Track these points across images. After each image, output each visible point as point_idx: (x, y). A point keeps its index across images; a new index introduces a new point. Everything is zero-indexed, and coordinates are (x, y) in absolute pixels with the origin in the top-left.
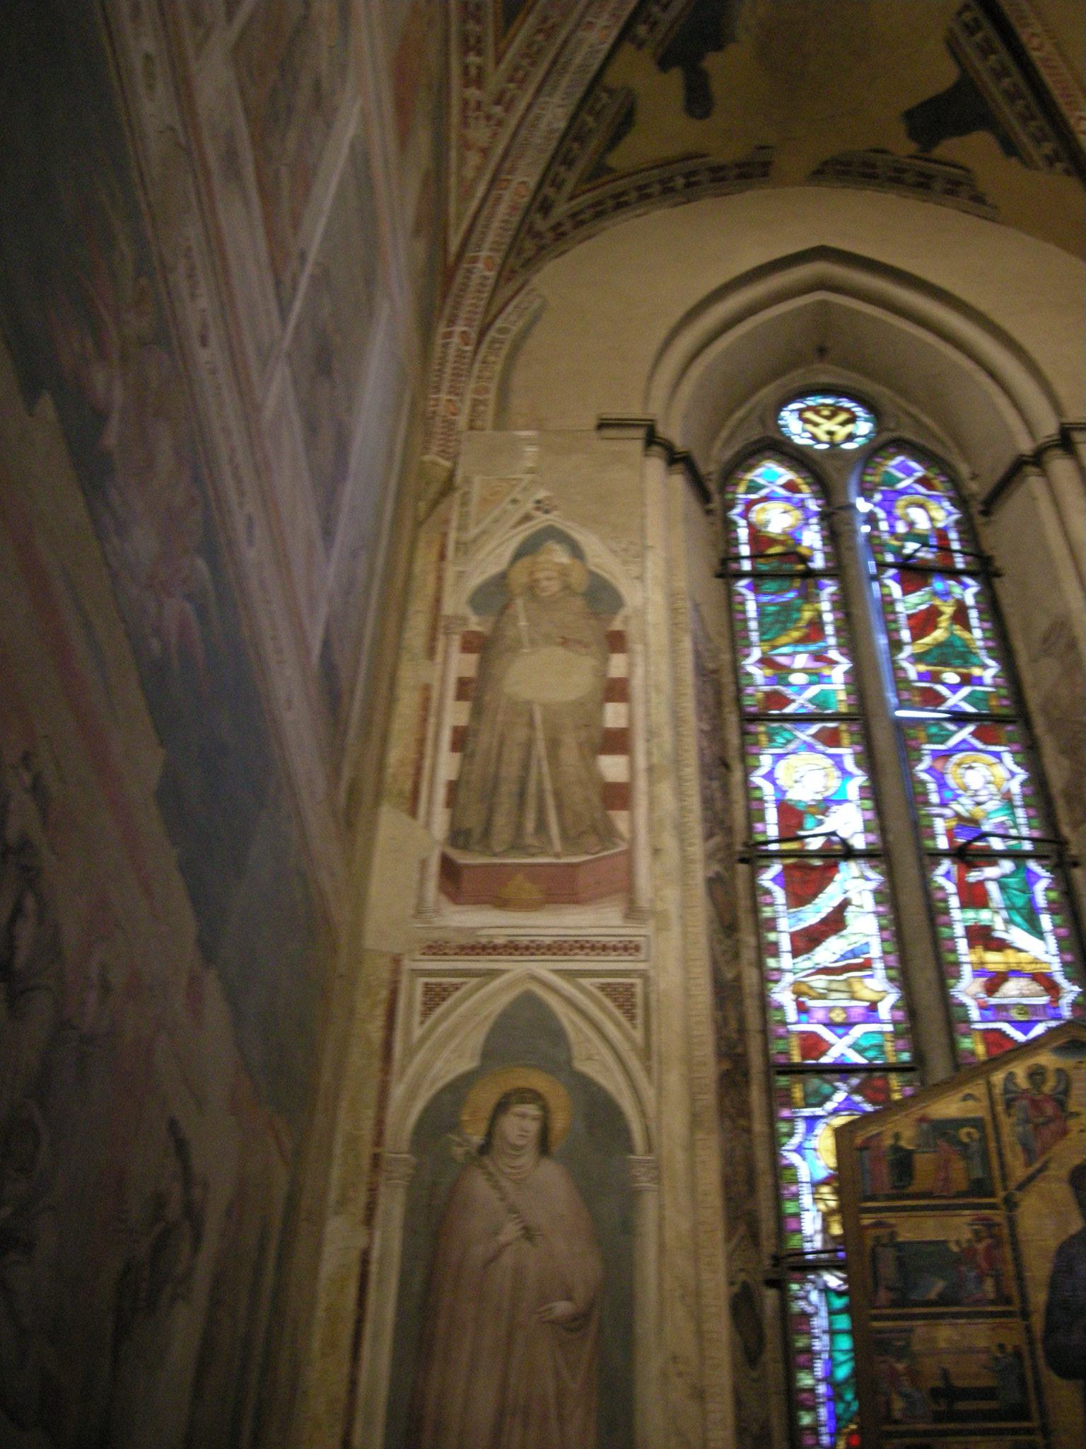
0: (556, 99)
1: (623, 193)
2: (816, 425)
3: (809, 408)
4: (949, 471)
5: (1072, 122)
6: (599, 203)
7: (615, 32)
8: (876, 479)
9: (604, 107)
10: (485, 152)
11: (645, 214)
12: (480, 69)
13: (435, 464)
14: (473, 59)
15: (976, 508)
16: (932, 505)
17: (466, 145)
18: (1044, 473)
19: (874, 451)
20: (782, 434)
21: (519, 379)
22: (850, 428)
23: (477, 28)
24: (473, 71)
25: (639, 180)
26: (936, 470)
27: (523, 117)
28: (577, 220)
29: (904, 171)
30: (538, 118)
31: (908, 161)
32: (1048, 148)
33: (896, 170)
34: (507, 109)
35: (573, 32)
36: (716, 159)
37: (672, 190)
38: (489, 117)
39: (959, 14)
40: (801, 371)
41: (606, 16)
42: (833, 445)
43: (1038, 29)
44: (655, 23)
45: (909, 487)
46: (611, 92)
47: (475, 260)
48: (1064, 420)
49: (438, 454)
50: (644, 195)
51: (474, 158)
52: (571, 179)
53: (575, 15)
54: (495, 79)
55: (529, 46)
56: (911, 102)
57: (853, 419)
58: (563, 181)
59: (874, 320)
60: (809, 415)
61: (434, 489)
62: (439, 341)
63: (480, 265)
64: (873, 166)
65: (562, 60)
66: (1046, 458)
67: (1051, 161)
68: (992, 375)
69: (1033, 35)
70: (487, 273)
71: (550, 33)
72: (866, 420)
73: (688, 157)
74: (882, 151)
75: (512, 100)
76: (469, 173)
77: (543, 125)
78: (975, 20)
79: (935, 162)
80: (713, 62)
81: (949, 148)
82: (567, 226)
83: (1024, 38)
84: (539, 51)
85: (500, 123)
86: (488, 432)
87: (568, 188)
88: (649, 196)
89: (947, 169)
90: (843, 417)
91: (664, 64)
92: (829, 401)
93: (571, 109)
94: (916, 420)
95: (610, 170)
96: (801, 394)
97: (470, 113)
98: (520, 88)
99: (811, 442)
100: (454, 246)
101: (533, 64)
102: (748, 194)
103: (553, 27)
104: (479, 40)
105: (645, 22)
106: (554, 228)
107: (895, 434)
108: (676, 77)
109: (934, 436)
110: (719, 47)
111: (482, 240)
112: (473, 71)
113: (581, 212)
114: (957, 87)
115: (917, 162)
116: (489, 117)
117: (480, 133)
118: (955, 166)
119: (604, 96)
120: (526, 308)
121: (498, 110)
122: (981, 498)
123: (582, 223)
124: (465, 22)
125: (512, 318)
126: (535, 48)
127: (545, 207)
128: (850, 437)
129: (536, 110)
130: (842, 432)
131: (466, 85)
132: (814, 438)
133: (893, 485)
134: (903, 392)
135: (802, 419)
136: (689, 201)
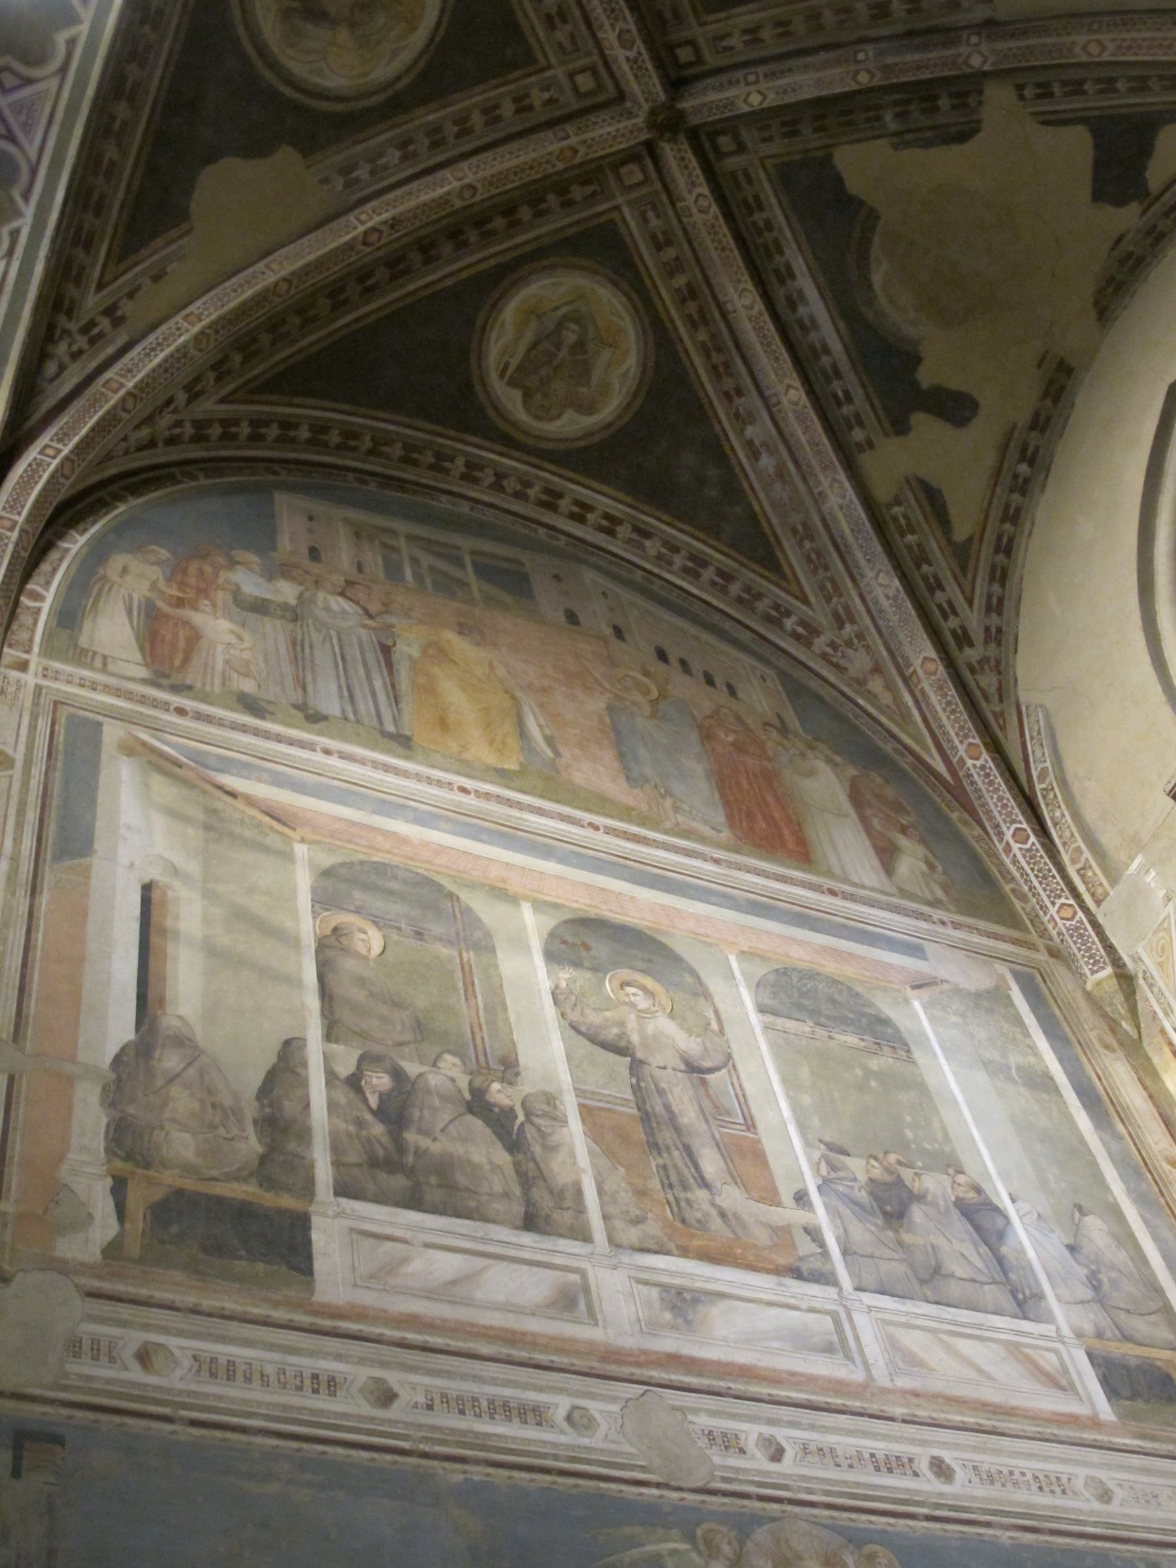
0: (870, 574)
1: (999, 538)
6: (993, 568)
7: (842, 476)
9: (905, 517)
10: (877, 669)
11: (1033, 524)
12: (802, 623)
13: (1098, 984)
14: (789, 623)
17: (860, 683)
21: (1090, 815)
23: (767, 601)
24: (800, 630)
25: (996, 512)
27: (869, 612)
28: (995, 606)
29: (1155, 227)
30: (876, 603)
31: (1145, 218)
33: (1149, 233)
34: (852, 621)
35: (820, 511)
36: (1024, 418)
37: (1026, 481)
38: (849, 643)
39: (1022, 97)
41: (822, 478)
44: (857, 415)
46: (897, 501)
47: (962, 762)
49: (1093, 972)
50: (1013, 516)
51: (876, 684)
52: (952, 591)
53: (808, 501)
54: (820, 615)
55: (809, 560)
56: (1084, 193)
58: (950, 603)
61: (1119, 999)
62: (1007, 861)
63: (969, 762)
64: (1130, 255)
65: (839, 540)
69: (1084, 48)
70: (978, 763)
71: (809, 533)
73: (1004, 449)
74: (1119, 240)
75: (847, 608)
76: (886, 698)
77: (885, 604)
79: (1163, 193)
80: (926, 377)
82: (994, 620)
84: (819, 555)
85: (860, 636)
86: (1112, 893)
87: (960, 602)
88: (1018, 511)
91: (900, 427)
93: (887, 566)
95: (970, 540)
97: (834, 660)
98: (841, 595)
100: (941, 768)
101: (827, 568)
102: (1079, 401)
103: (805, 525)
104: (777, 607)
105: (851, 428)
106: (987, 641)
108: (919, 419)
110: (919, 360)
111: (950, 741)
112: (800, 630)
113: (989, 597)
116: (849, 643)
117: (859, 662)
119: (896, 510)
120: (1039, 733)
121: (848, 628)
123: (1001, 601)
124: (753, 610)
125: (1039, 753)
126: (814, 556)
127: (963, 639)
129: (868, 598)
131: (808, 645)
136: (1048, 471)
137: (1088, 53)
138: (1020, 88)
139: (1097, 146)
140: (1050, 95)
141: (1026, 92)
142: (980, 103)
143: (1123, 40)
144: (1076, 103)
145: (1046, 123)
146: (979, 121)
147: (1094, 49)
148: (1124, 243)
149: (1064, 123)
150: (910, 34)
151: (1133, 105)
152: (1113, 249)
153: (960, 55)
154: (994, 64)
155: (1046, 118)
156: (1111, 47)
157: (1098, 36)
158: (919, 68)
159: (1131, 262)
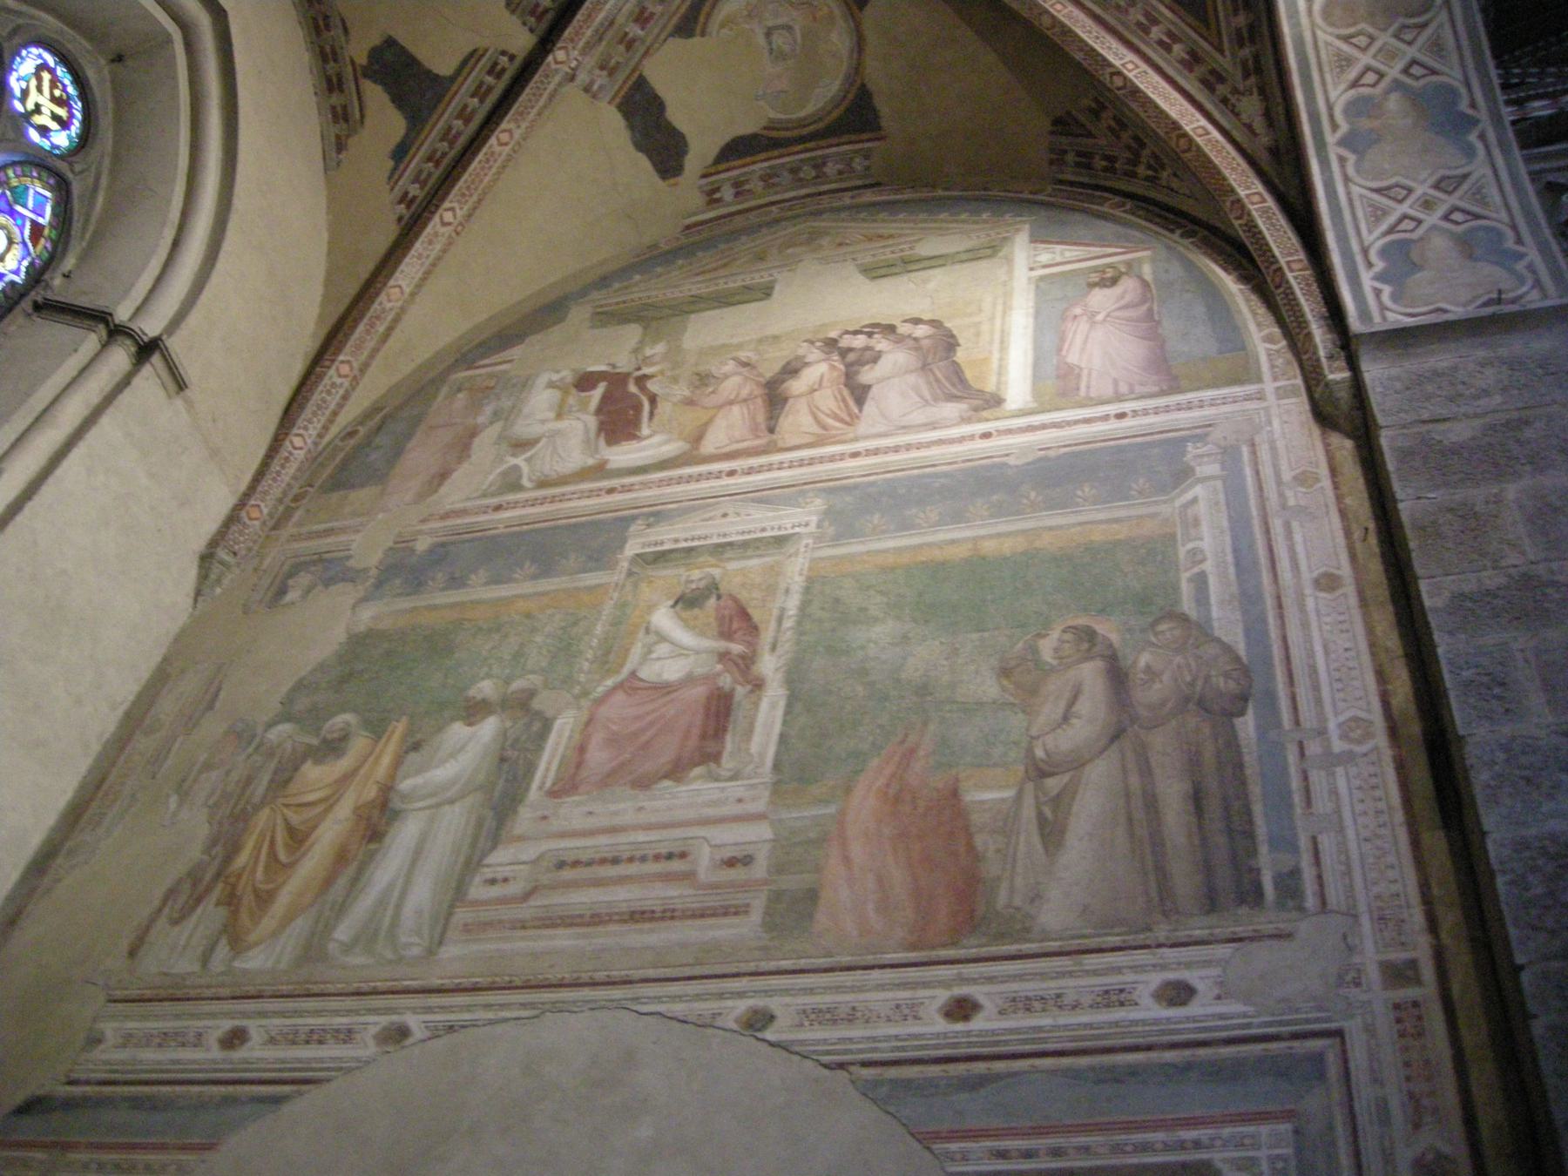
2: (39, 89)
3: (52, 71)
4: (60, 249)
5: (447, 204)
8: (14, 182)
15: (38, 295)
16: (17, 251)
18: (105, 346)
19: (41, 163)
20: (12, 62)
22: (53, 125)
26: (54, 235)
29: (335, 61)
31: (348, 59)
32: (414, 190)
33: (334, 53)
39: (503, 53)
40: (88, 46)
42: (27, 116)
43: (517, 134)
45: (23, 217)
48: (164, 337)
57: (64, 124)
59: (174, 96)
60: (46, 76)
64: (328, 27)
66: (120, 338)
67: (404, 198)
68: (176, 244)
72: (69, 137)
78: (504, 70)
81: (375, 95)
83: (504, 125)
89: (356, 104)
90: (62, 112)
92: (71, 90)
94: (95, 188)
96: (64, 59)
99: (18, 93)
107: (70, 176)
109: (87, 221)
114: (435, 78)
115: (350, 69)
118: (361, 110)
122: (50, 295)
128: (44, 131)
130: (43, 120)
132: (23, 99)
133: (17, 202)
134: (116, 158)
135: (37, 74)
137: (505, 131)
138: (512, 58)
139: (429, 72)
140: (490, 72)
141: (505, 59)
142: (524, 24)
143: (495, 161)
144: (470, 84)
145: (471, 55)
146: (513, 12)
147: (504, 137)
148: (340, 31)
149: (464, 63)
150: (612, 23)
151: (438, 120)
152: (343, 21)
153: (574, 48)
154: (548, 65)
155: (476, 56)
156: (497, 149)
157: (510, 146)
158: (589, 16)
159: (321, 23)
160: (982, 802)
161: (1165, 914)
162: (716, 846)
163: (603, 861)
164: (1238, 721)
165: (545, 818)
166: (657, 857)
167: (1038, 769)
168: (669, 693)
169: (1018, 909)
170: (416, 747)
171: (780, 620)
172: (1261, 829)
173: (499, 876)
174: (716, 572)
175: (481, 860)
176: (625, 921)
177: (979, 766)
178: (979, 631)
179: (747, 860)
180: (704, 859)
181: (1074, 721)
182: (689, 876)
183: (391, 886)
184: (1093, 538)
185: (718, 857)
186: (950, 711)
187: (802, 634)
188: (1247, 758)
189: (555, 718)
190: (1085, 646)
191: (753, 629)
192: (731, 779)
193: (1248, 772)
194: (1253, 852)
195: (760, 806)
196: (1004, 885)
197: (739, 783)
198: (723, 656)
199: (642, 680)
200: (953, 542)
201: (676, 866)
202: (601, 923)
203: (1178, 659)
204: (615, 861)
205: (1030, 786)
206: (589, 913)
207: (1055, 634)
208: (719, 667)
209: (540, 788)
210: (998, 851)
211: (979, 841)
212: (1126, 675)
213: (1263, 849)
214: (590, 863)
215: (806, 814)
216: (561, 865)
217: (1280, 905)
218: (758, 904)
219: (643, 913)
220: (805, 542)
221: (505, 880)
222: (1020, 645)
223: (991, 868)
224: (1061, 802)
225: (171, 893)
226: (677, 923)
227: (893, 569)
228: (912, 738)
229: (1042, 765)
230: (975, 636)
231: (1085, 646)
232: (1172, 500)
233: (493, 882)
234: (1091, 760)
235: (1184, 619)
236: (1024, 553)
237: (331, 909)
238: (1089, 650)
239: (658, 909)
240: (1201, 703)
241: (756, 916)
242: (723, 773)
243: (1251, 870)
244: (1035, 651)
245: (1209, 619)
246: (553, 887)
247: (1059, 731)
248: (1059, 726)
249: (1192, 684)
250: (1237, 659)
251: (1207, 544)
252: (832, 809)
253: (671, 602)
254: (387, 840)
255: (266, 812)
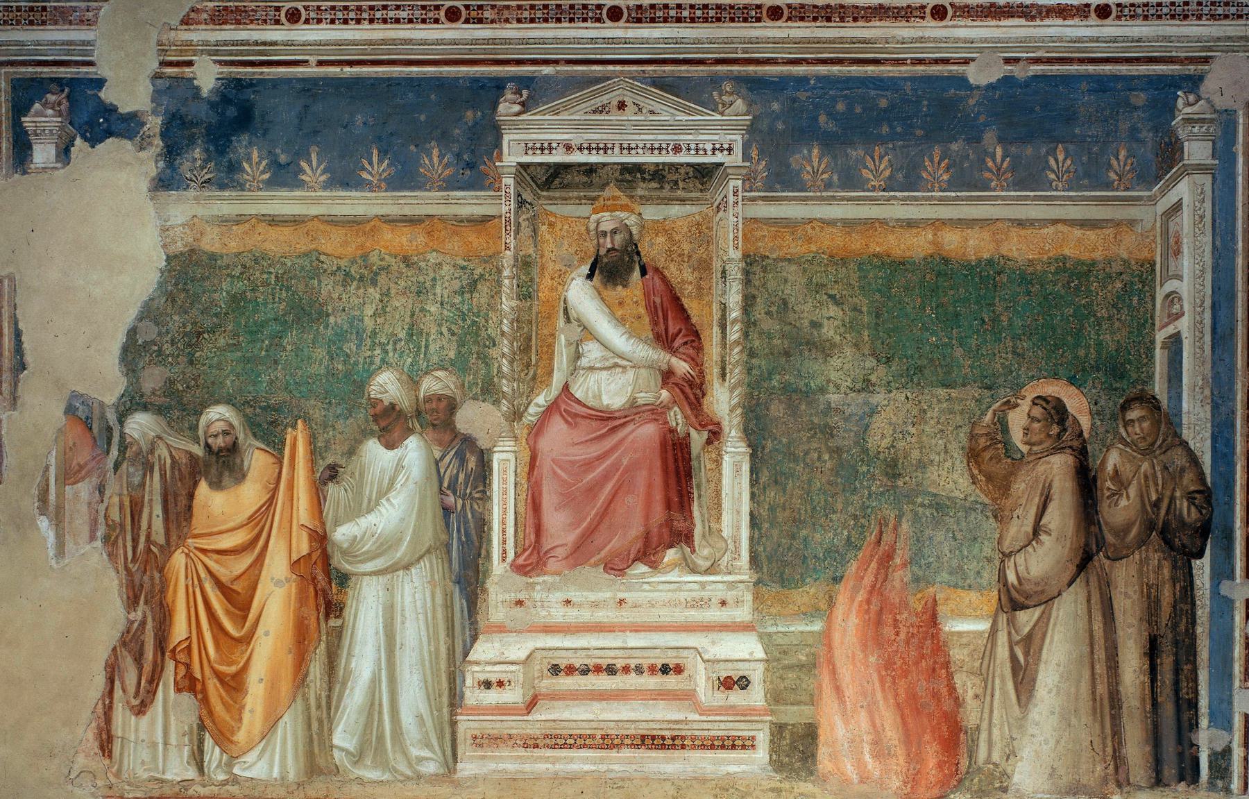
160: (960, 634)
161: (1119, 785)
162: (708, 661)
163: (598, 669)
164: (1196, 563)
165: (520, 603)
166: (652, 669)
167: (1011, 600)
168: (614, 430)
169: (996, 765)
170: (333, 474)
171: (723, 327)
172: (1203, 703)
173: (494, 678)
174: (632, 220)
175: (466, 654)
176: (638, 747)
177: (956, 586)
178: (947, 386)
179: (743, 683)
180: (701, 681)
181: (1043, 537)
182: (687, 697)
183: (375, 681)
184: (1067, 252)
185: (715, 676)
186: (922, 505)
187: (752, 354)
188: (1199, 613)
189: (490, 451)
190: (1055, 430)
191: (695, 336)
192: (707, 572)
193: (1199, 630)
194: (1194, 725)
195: (743, 613)
196: (984, 736)
197: (718, 578)
198: (667, 376)
199: (578, 402)
200: (910, 224)
201: (671, 681)
202: (611, 747)
203: (1145, 466)
204: (611, 670)
205: (1003, 619)
206: (599, 733)
207: (1025, 405)
208: (665, 394)
209: (504, 559)
210: (977, 696)
211: (958, 680)
212: (1095, 479)
213: (1204, 722)
214: (585, 671)
215: (792, 629)
216: (555, 670)
217: (1212, 786)
218: (763, 738)
219: (653, 738)
220: (732, 183)
221: (500, 684)
222: (988, 417)
223: (971, 715)
224: (1031, 643)
225: (112, 672)
226: (687, 753)
227: (844, 261)
228: (887, 537)
229: (1014, 594)
230: (942, 392)
231: (1055, 430)
232: (1153, 200)
233: (487, 685)
234: (1059, 594)
235: (1152, 403)
236: (990, 262)
237: (319, 707)
238: (1059, 436)
239: (667, 734)
240: (1166, 535)
241: (761, 754)
242: (700, 562)
243: (1192, 745)
244: (1002, 425)
245: (1179, 414)
246: (555, 696)
247: (1030, 549)
248: (1030, 543)
249: (1156, 505)
250: (1201, 476)
251: (1184, 288)
252: (817, 626)
253: (585, 269)
254: (348, 612)
255: (179, 560)
